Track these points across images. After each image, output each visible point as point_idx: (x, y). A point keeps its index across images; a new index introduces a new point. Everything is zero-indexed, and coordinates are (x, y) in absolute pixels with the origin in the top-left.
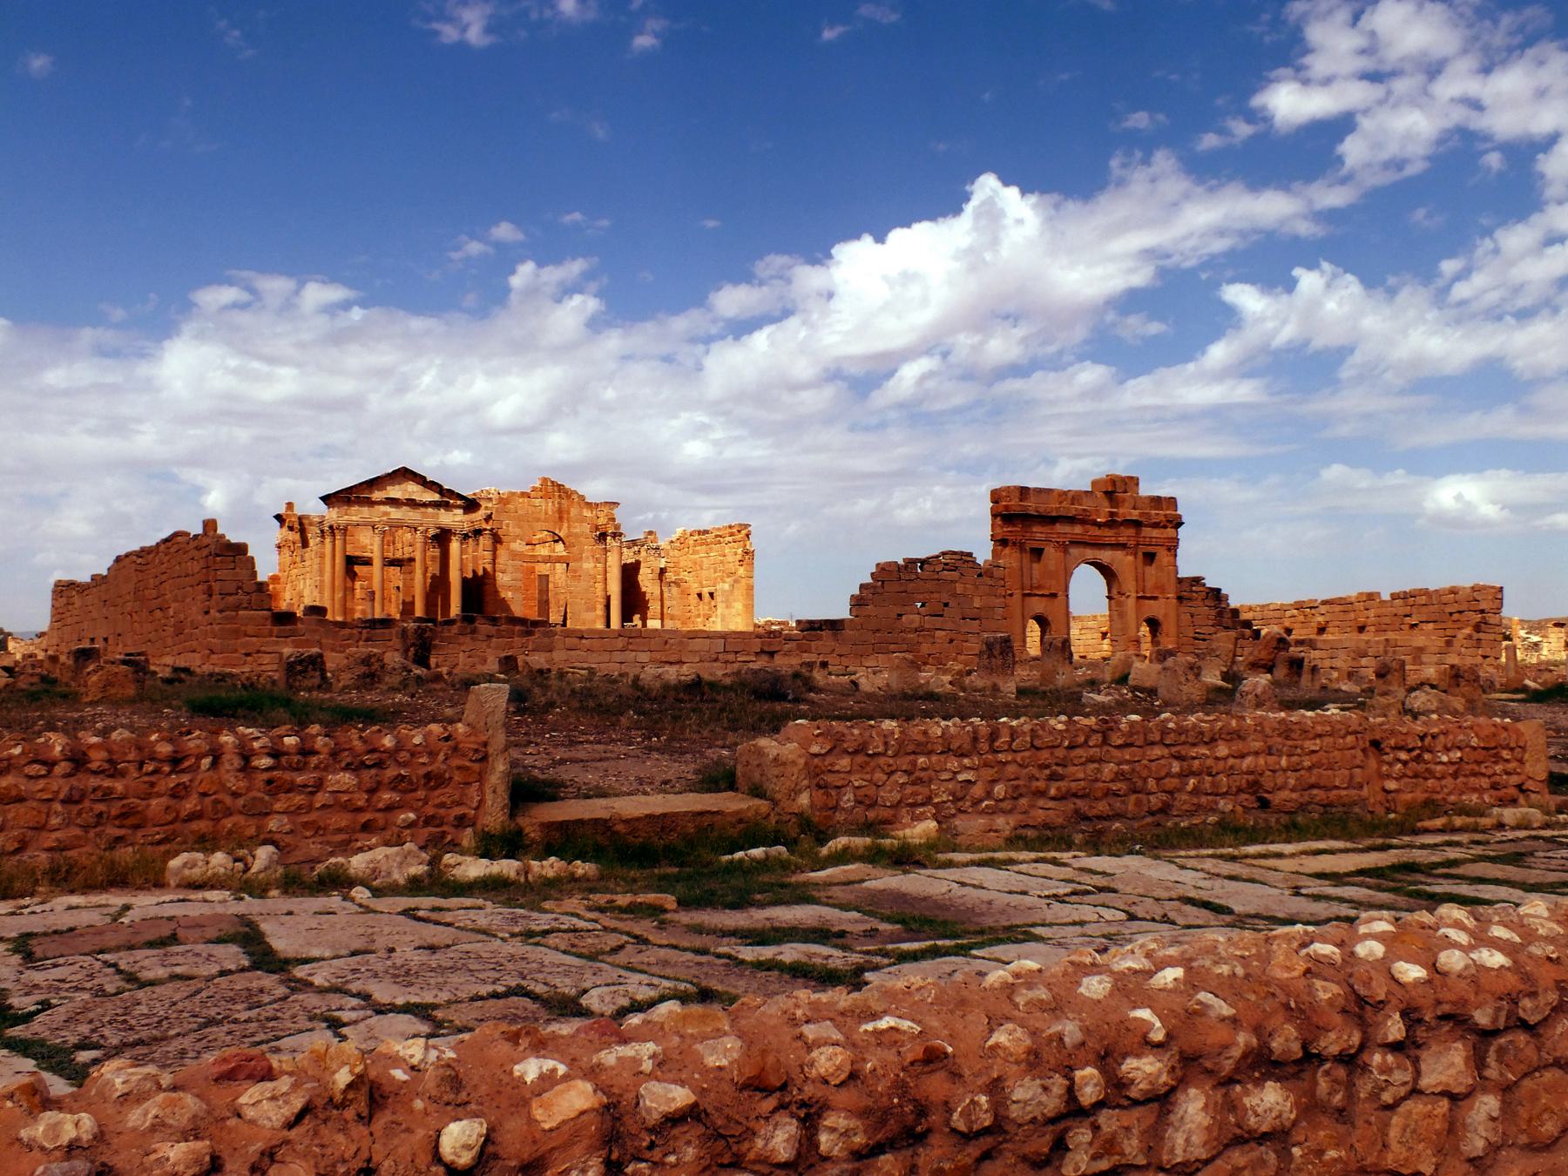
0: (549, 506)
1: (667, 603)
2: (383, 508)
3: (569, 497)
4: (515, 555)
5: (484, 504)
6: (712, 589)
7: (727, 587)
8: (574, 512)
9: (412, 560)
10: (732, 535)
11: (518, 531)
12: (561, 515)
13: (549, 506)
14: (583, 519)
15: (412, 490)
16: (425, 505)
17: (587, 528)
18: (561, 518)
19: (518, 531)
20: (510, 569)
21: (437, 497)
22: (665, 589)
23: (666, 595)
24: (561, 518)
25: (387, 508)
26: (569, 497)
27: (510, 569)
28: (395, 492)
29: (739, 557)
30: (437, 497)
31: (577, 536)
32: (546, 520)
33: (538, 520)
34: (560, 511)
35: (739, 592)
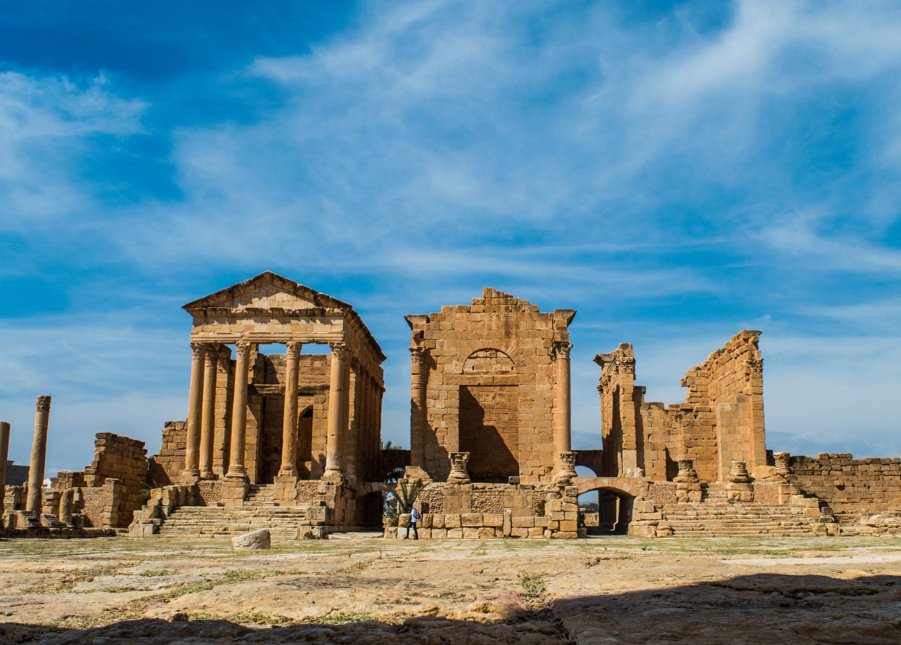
0: (494, 321)
1: (647, 430)
2: (245, 322)
4: (448, 379)
7: (728, 407)
8: (524, 325)
9: (328, 388)
11: (453, 350)
12: (508, 331)
13: (494, 321)
14: (534, 334)
15: (284, 300)
16: (295, 315)
17: (540, 344)
18: (508, 334)
19: (453, 350)
20: (443, 395)
21: (311, 306)
22: (643, 412)
23: (645, 420)
24: (508, 334)
25: (251, 322)
27: (443, 395)
28: (263, 303)
30: (311, 306)
31: (528, 353)
32: (489, 337)
33: (480, 337)
34: (507, 325)
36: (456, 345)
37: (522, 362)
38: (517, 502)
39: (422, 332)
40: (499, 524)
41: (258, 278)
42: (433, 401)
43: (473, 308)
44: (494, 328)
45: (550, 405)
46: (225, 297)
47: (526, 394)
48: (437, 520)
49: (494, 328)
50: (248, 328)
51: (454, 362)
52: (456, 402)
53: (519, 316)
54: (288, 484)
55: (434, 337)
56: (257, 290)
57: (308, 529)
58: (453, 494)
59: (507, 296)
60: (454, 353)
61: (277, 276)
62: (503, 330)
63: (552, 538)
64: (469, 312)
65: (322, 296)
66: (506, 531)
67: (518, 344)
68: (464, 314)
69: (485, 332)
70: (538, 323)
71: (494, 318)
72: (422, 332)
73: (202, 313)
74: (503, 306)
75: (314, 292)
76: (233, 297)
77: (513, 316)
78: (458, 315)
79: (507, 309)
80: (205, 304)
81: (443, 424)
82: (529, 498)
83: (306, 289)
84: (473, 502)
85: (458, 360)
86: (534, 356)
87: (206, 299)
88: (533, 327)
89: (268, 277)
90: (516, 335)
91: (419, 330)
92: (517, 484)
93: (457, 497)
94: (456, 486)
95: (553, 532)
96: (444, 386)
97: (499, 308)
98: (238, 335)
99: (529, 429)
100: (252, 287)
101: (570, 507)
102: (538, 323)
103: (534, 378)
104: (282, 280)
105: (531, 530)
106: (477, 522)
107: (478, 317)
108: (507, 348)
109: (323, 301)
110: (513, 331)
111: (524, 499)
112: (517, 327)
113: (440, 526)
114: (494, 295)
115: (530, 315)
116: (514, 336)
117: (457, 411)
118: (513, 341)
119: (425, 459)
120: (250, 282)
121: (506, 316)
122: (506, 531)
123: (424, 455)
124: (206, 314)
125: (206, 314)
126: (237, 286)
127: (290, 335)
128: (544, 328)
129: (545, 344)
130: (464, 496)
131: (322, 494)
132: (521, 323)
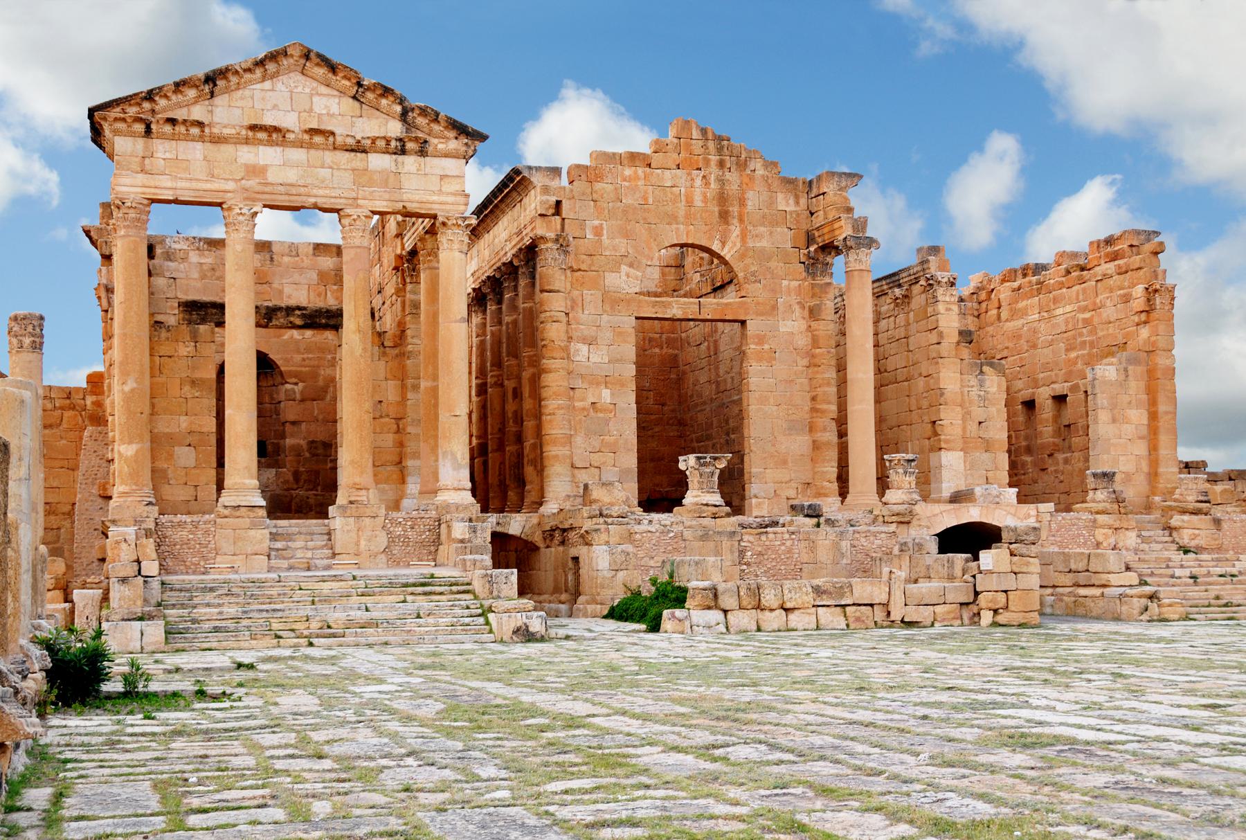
0: (697, 189)
2: (247, 155)
3: (742, 165)
4: (613, 301)
5: (537, 179)
6: (1060, 388)
8: (754, 200)
10: (1114, 257)
11: (622, 245)
13: (697, 189)
16: (358, 148)
17: (784, 238)
18: (724, 216)
19: (622, 245)
26: (742, 165)
29: (1139, 303)
31: (764, 256)
33: (672, 219)
34: (722, 198)
35: (1136, 386)
36: (627, 235)
37: (753, 274)
38: (824, 554)
39: (558, 203)
40: (883, 598)
41: (273, 57)
42: (584, 348)
43: (657, 160)
44: (698, 202)
45: (805, 362)
46: (192, 93)
47: (761, 340)
48: (769, 598)
49: (698, 202)
50: (255, 171)
51: (624, 268)
52: (630, 351)
53: (746, 180)
54: (367, 520)
55: (582, 216)
56: (267, 84)
57: (518, 620)
58: (705, 537)
59: (719, 139)
60: (623, 251)
61: (319, 55)
62: (717, 209)
63: (995, 624)
64: (649, 165)
65: (423, 111)
66: (896, 615)
67: (743, 236)
68: (640, 171)
69: (681, 213)
70: (780, 196)
71: (698, 182)
72: (558, 203)
73: (140, 128)
74: (714, 159)
75: (401, 101)
76: (212, 95)
77: (733, 177)
78: (628, 172)
79: (721, 164)
80: (147, 105)
81: (606, 395)
82: (845, 545)
83: (386, 91)
84: (742, 553)
85: (631, 265)
86: (773, 264)
87: (150, 96)
88: (772, 202)
89: (296, 52)
90: (741, 220)
91: (553, 199)
92: (818, 516)
93: (712, 544)
94: (708, 522)
95: (996, 611)
96: (605, 317)
97: (707, 162)
98: (231, 186)
99: (766, 408)
100: (259, 72)
101: (1028, 564)
102: (780, 196)
103: (774, 307)
104: (333, 68)
105: (938, 609)
106: (842, 596)
107: (668, 177)
108: (723, 244)
109: (421, 121)
110: (734, 210)
111: (836, 546)
112: (742, 202)
113: (775, 605)
114: (696, 134)
115: (765, 179)
116: (735, 221)
117: (631, 370)
118: (735, 231)
119: (572, 466)
120: (260, 63)
121: (721, 181)
122: (896, 615)
123: (571, 457)
124: (148, 131)
125: (148, 131)
126: (223, 73)
127: (354, 195)
128: (791, 207)
129: (794, 239)
130: (726, 544)
131: (462, 541)
132: (750, 195)
